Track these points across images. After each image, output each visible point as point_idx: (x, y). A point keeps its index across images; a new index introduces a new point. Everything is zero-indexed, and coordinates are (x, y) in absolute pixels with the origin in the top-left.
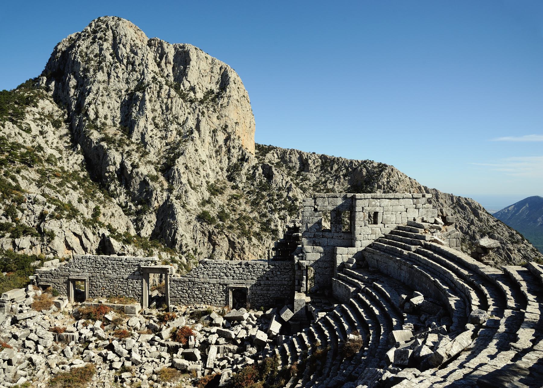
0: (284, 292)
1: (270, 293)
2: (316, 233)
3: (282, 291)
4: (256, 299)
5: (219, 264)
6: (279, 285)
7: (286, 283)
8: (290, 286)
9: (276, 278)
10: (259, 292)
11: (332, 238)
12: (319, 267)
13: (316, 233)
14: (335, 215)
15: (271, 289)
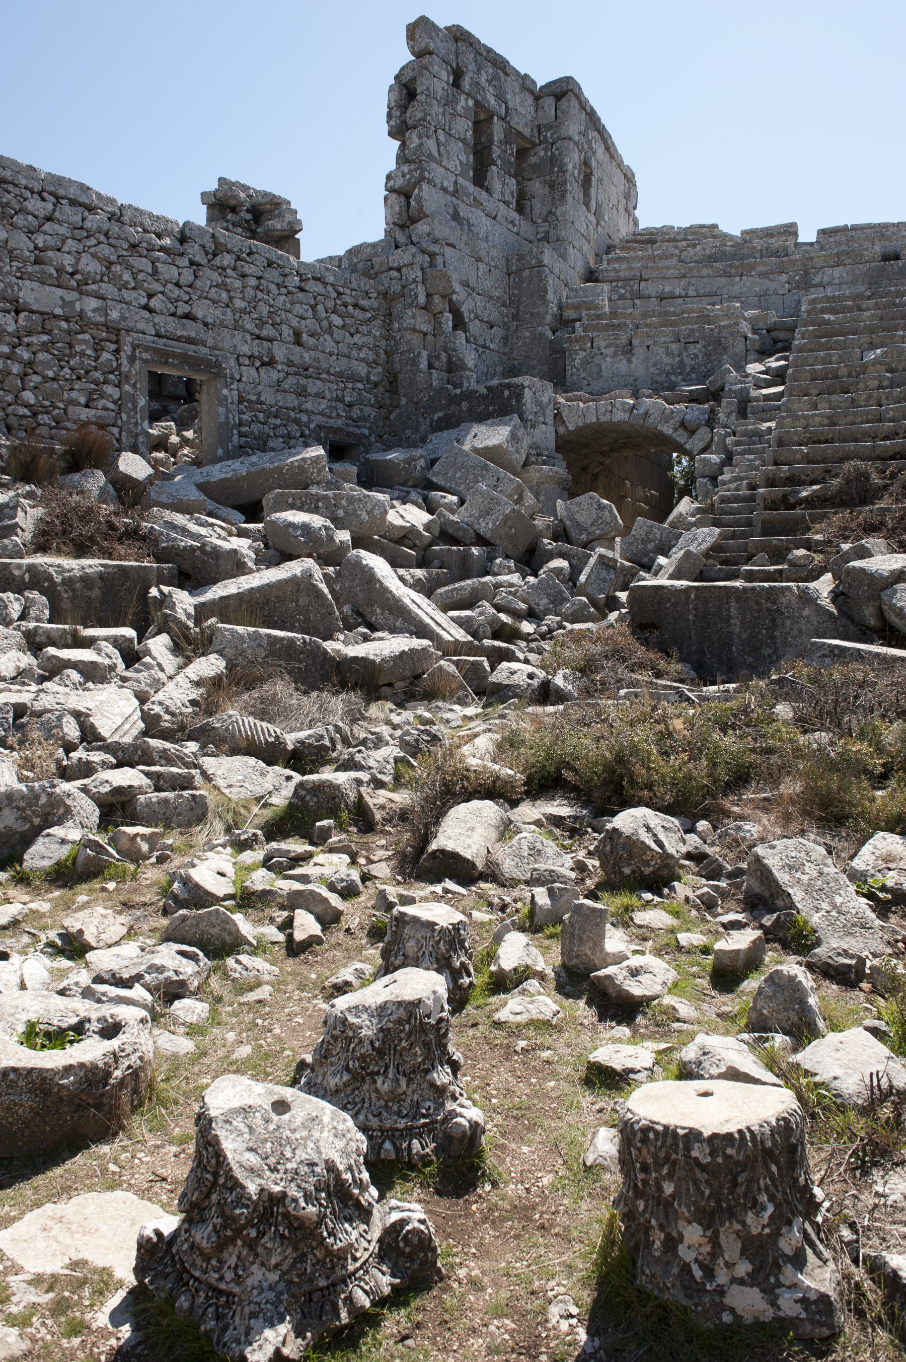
0: (356, 412)
1: (308, 405)
2: (461, 180)
3: (350, 406)
4: (256, 428)
5: (73, 203)
6: (340, 375)
7: (362, 369)
8: (376, 385)
9: (328, 343)
10: (268, 397)
11: (494, 218)
12: (477, 317)
13: (461, 180)
14: (502, 137)
15: (312, 390)
